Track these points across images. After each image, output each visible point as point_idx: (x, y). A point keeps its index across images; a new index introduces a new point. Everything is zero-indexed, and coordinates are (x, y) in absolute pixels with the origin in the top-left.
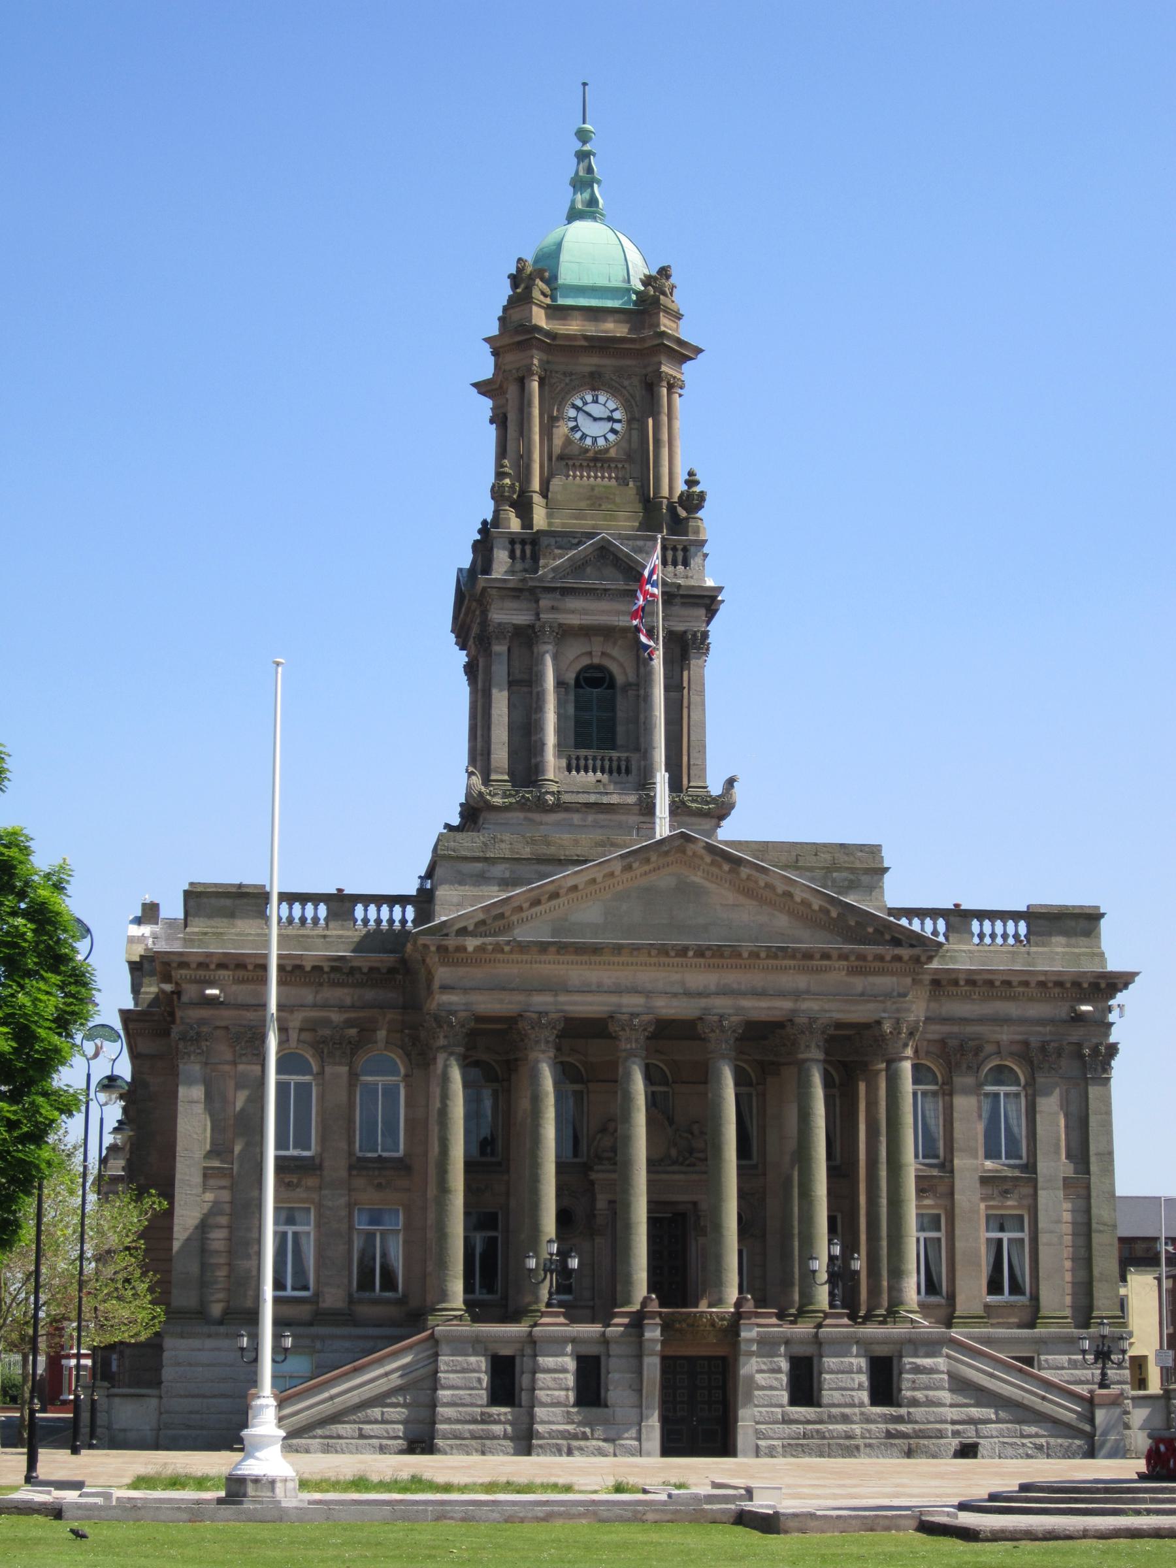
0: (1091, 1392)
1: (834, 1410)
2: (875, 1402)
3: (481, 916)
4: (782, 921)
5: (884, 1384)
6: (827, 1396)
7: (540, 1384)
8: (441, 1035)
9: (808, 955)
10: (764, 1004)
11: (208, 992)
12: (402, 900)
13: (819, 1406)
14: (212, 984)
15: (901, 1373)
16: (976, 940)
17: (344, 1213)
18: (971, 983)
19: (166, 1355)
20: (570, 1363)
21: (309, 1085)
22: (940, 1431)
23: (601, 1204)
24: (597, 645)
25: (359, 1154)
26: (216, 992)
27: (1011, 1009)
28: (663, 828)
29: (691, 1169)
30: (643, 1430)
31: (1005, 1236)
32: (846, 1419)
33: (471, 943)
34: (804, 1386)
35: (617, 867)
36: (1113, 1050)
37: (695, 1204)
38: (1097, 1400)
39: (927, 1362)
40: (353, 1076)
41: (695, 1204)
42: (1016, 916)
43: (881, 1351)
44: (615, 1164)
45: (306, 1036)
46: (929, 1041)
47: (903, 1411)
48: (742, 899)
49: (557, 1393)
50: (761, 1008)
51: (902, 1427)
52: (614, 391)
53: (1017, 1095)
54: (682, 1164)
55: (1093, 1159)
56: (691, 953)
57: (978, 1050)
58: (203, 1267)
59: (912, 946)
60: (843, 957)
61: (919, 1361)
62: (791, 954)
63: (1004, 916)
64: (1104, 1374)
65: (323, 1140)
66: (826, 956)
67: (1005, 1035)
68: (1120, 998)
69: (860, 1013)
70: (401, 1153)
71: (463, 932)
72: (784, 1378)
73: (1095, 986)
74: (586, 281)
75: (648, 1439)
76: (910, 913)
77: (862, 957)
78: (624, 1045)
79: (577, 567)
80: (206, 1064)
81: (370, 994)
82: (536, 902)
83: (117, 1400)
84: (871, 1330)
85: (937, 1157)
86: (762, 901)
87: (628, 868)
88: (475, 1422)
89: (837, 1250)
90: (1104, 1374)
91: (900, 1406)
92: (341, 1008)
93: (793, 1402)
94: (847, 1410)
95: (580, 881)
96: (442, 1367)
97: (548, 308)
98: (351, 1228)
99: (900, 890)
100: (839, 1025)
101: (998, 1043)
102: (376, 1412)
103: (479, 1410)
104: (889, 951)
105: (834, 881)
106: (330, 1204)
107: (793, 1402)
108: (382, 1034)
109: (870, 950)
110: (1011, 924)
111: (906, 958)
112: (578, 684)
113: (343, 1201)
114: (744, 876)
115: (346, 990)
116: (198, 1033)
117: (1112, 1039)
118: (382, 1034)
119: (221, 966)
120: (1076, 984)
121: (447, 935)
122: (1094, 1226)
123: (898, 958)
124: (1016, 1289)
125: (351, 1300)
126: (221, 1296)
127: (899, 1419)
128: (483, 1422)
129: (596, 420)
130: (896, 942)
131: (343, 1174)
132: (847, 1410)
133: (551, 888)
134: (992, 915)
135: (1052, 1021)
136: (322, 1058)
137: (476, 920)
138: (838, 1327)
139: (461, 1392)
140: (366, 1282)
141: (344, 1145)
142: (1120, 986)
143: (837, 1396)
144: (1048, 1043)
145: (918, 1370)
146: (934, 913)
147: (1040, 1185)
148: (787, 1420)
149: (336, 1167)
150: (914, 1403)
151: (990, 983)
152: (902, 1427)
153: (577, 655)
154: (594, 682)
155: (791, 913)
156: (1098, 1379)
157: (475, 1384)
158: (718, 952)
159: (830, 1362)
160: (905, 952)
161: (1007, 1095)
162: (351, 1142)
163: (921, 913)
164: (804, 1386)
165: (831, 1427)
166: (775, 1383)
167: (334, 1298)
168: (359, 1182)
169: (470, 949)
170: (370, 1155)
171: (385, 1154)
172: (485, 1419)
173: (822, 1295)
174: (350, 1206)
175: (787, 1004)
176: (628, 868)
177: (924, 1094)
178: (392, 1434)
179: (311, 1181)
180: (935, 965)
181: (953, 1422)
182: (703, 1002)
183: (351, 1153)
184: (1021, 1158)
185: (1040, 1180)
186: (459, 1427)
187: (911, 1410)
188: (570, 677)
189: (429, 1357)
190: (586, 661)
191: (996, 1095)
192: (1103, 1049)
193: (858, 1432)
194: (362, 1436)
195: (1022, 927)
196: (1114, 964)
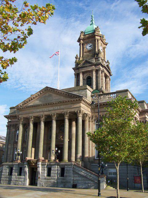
4: (62, 97)
18: (104, 105)
24: (88, 74)
43: (62, 167)
47: (64, 178)
50: (59, 112)
52: (90, 42)
60: (68, 101)
74: (89, 31)
77: (71, 101)
79: (84, 64)
89: (57, 149)
97: (84, 35)
104: (75, 99)
109: (72, 100)
112: (87, 79)
123: (77, 100)
127: (64, 179)
129: (88, 47)
130: (76, 97)
150: (66, 176)
153: (86, 76)
154: (89, 79)
155: (63, 96)
160: (77, 99)
188: (86, 78)
190: (87, 76)
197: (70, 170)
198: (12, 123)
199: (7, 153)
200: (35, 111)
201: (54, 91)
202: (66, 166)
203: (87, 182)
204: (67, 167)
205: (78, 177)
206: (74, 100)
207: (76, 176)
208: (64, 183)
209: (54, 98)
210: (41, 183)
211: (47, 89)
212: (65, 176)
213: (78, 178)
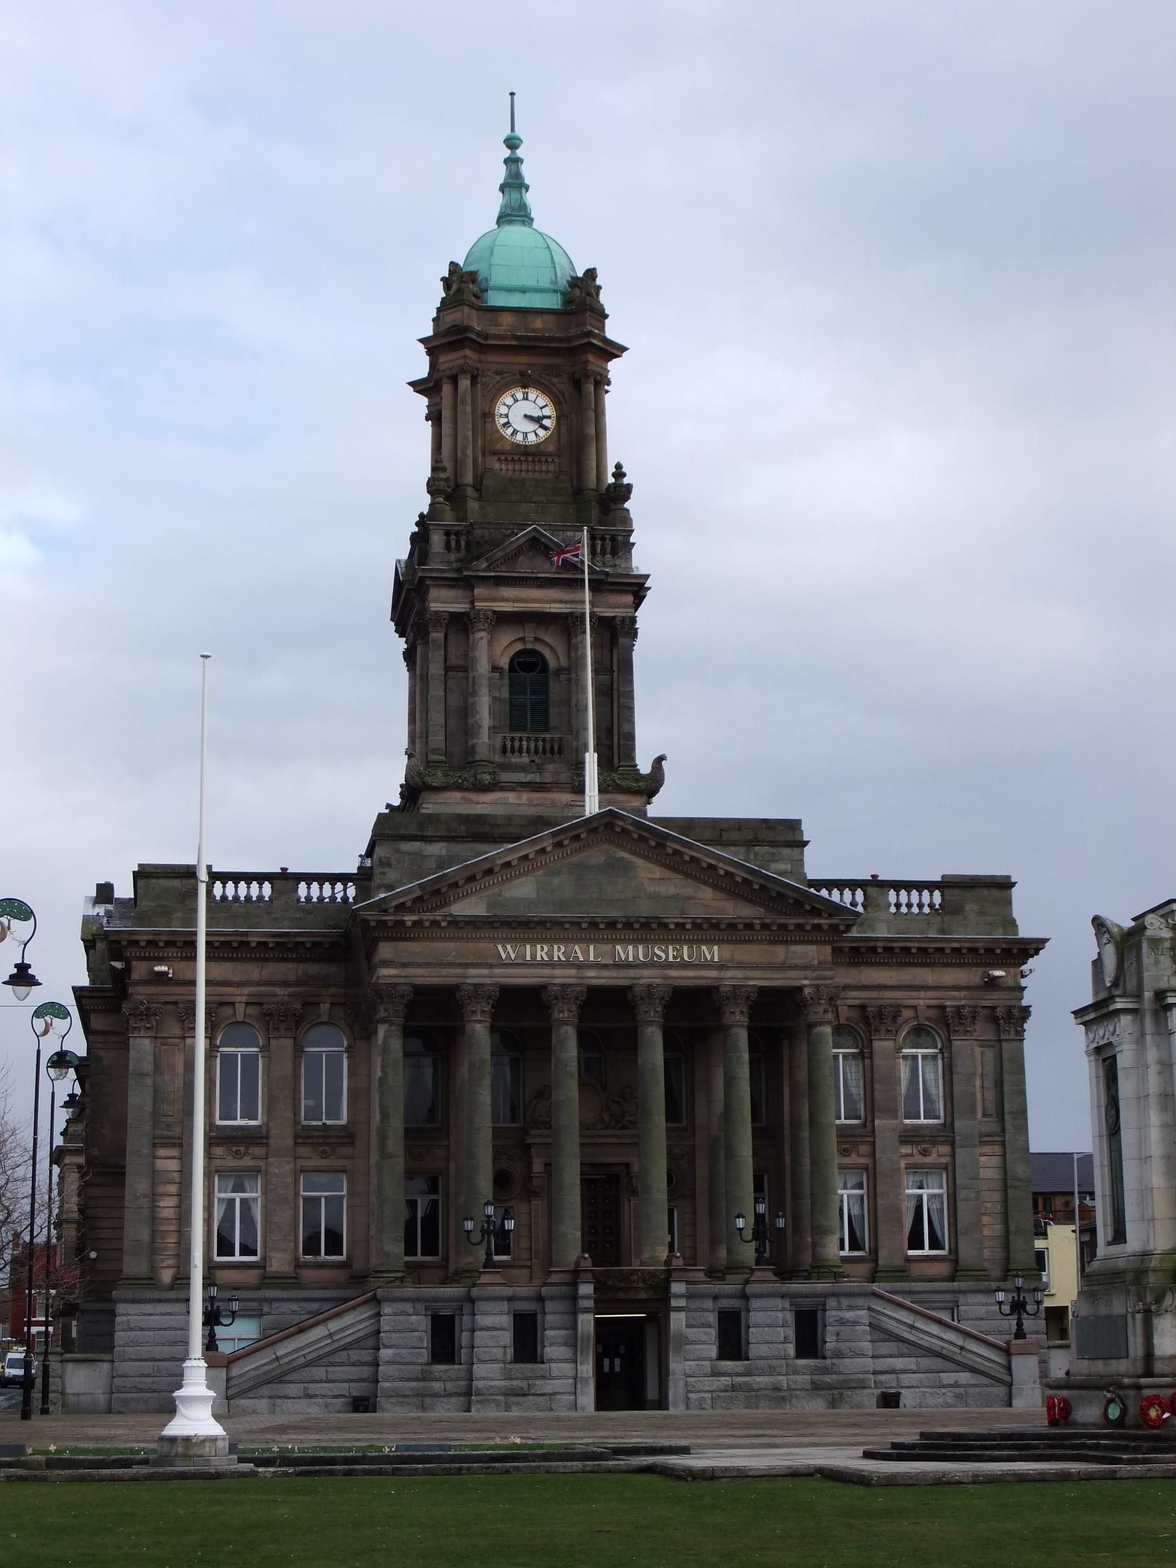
0: (1008, 1343)
1: (761, 1363)
2: (800, 1354)
3: (419, 893)
4: (707, 894)
5: (808, 1337)
6: (754, 1350)
7: (477, 1342)
8: (382, 1008)
9: (732, 926)
10: (691, 973)
11: (157, 969)
12: (344, 878)
13: (748, 1359)
14: (161, 960)
15: (825, 1326)
16: (893, 909)
17: (289, 1180)
18: (889, 950)
19: (118, 1319)
20: (506, 1321)
21: (254, 1057)
22: (863, 1380)
23: (537, 1167)
25: (304, 1123)
26: (164, 968)
27: (925, 975)
28: (592, 804)
29: (624, 1132)
30: (579, 1386)
31: (925, 1192)
32: (772, 1371)
33: (409, 918)
34: (732, 1341)
35: (548, 844)
36: (1025, 1012)
37: (627, 1165)
38: (1012, 1351)
39: (850, 1315)
40: (298, 1051)
41: (627, 1165)
42: (930, 886)
44: (550, 1128)
45: (252, 1010)
46: (850, 1006)
47: (829, 1361)
48: (667, 873)
49: (495, 1350)
51: (827, 1379)
53: (934, 1057)
54: (614, 1128)
55: (1007, 1117)
56: (620, 926)
57: (896, 1016)
58: (154, 1233)
59: (831, 916)
60: (765, 927)
61: (842, 1314)
62: (715, 925)
63: (920, 886)
64: (1020, 1325)
65: (270, 1110)
66: (749, 926)
67: (923, 1000)
68: (1032, 963)
69: (779, 980)
70: (344, 1121)
71: (401, 908)
72: (713, 1333)
73: (1007, 952)
75: (583, 1394)
76: (830, 884)
77: (783, 927)
78: (557, 1015)
80: (156, 1038)
81: (313, 969)
82: (472, 879)
83: (70, 1366)
84: (795, 1287)
85: (859, 1118)
86: (688, 875)
87: (559, 845)
88: (417, 1380)
90: (1020, 1325)
91: (824, 1358)
92: (285, 984)
93: (722, 1356)
94: (774, 1363)
95: (513, 857)
96: (385, 1328)
98: (297, 1194)
99: (818, 863)
100: (763, 991)
101: (915, 1007)
102: (320, 1372)
103: (419, 1368)
105: (756, 854)
106: (276, 1171)
107: (722, 1356)
108: (325, 1007)
109: (792, 921)
110: (926, 893)
111: (826, 927)
113: (289, 1168)
114: (670, 851)
115: (290, 965)
116: (148, 1009)
117: (1024, 1003)
118: (325, 1007)
119: (170, 944)
120: (990, 951)
121: (386, 911)
122: (1009, 1182)
123: (817, 927)
124: (935, 1244)
125: (298, 1265)
126: (171, 1262)
127: (825, 1371)
128: (424, 1379)
130: (816, 912)
131: (289, 1142)
132: (774, 1363)
133: (487, 866)
134: (909, 886)
135: (968, 988)
136: (268, 1029)
137: (414, 896)
138: (764, 1281)
139: (403, 1351)
140: (311, 1246)
141: (290, 1115)
142: (1032, 952)
143: (763, 1350)
144: (963, 1006)
145: (842, 1322)
146: (853, 885)
147: (957, 1143)
148: (716, 1373)
149: (282, 1137)
150: (839, 1355)
151: (907, 950)
152: (827, 1379)
155: (715, 887)
156: (1014, 1328)
157: (417, 1344)
158: (646, 924)
159: (756, 1317)
161: (924, 1057)
162: (296, 1112)
163: (840, 884)
164: (732, 1341)
165: (758, 1379)
166: (704, 1338)
167: (279, 1263)
168: (304, 1151)
169: (409, 924)
170: (314, 1123)
171: (329, 1122)
172: (425, 1377)
173: (748, 1252)
174: (296, 1174)
175: (714, 974)
176: (559, 845)
177: (845, 1056)
178: (336, 1393)
179: (258, 1151)
180: (854, 933)
181: (875, 1373)
182: (632, 973)
183: (296, 1122)
184: (938, 1118)
185: (958, 1138)
186: (400, 1384)
187: (834, 1361)
189: (370, 1317)
191: (915, 1057)
192: (1015, 1012)
193: (785, 1383)
194: (309, 1396)
195: (937, 897)
196: (1026, 931)
197: (855, 1323)
198: (176, 990)
199: (154, 1208)
200: (507, 951)
201: (661, 846)
202: (831, 1303)
203: (947, 1378)
204: (839, 1309)
205: (901, 1356)
206: (800, 927)
207: (886, 1348)
208: (831, 1387)
209: (651, 889)
210: (690, 1395)
211: (610, 826)
212: (828, 1354)
213: (898, 1363)
